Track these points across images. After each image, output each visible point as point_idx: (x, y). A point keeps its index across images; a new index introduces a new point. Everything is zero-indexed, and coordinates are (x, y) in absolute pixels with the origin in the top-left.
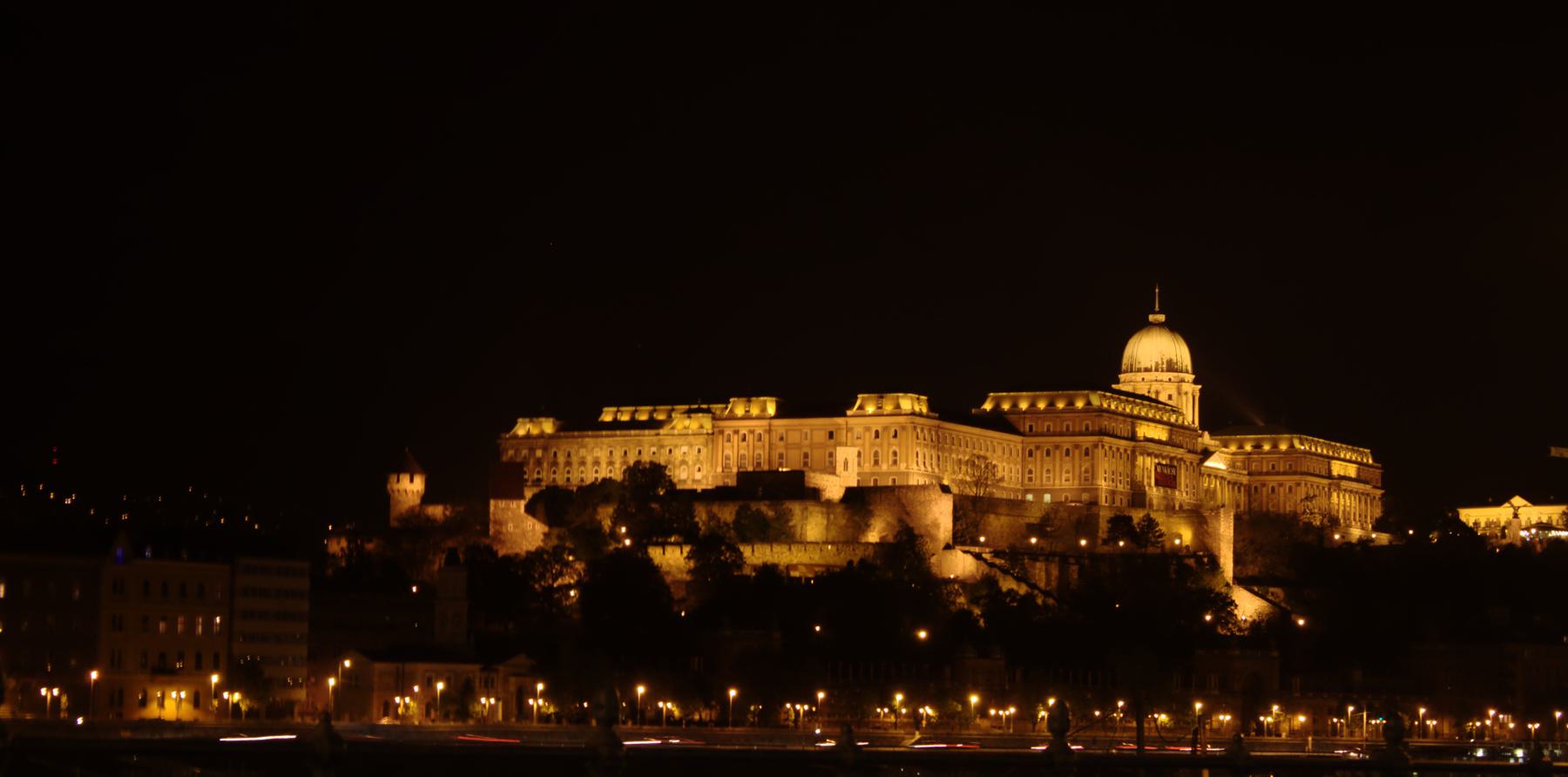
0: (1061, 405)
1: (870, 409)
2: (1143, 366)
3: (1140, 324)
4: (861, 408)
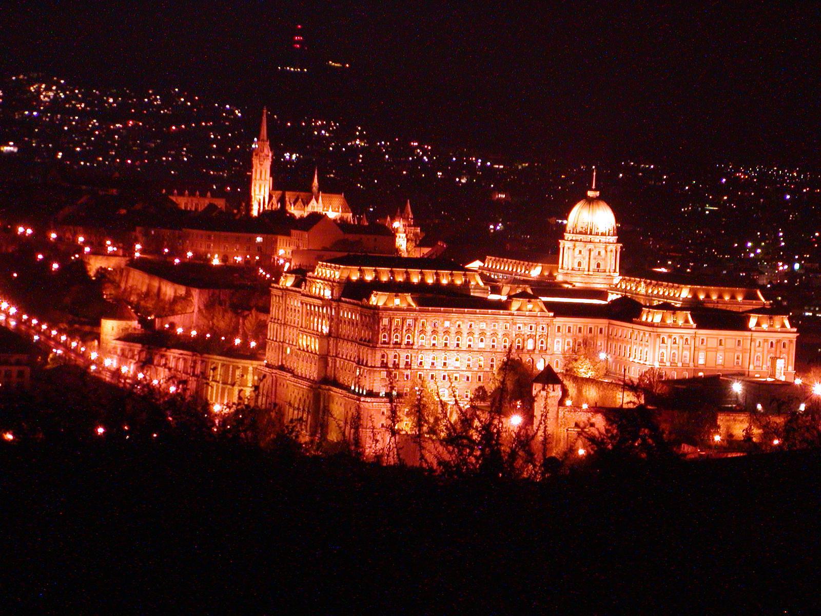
0: (727, 298)
1: (765, 326)
2: (600, 231)
3: (578, 195)
4: (758, 324)
